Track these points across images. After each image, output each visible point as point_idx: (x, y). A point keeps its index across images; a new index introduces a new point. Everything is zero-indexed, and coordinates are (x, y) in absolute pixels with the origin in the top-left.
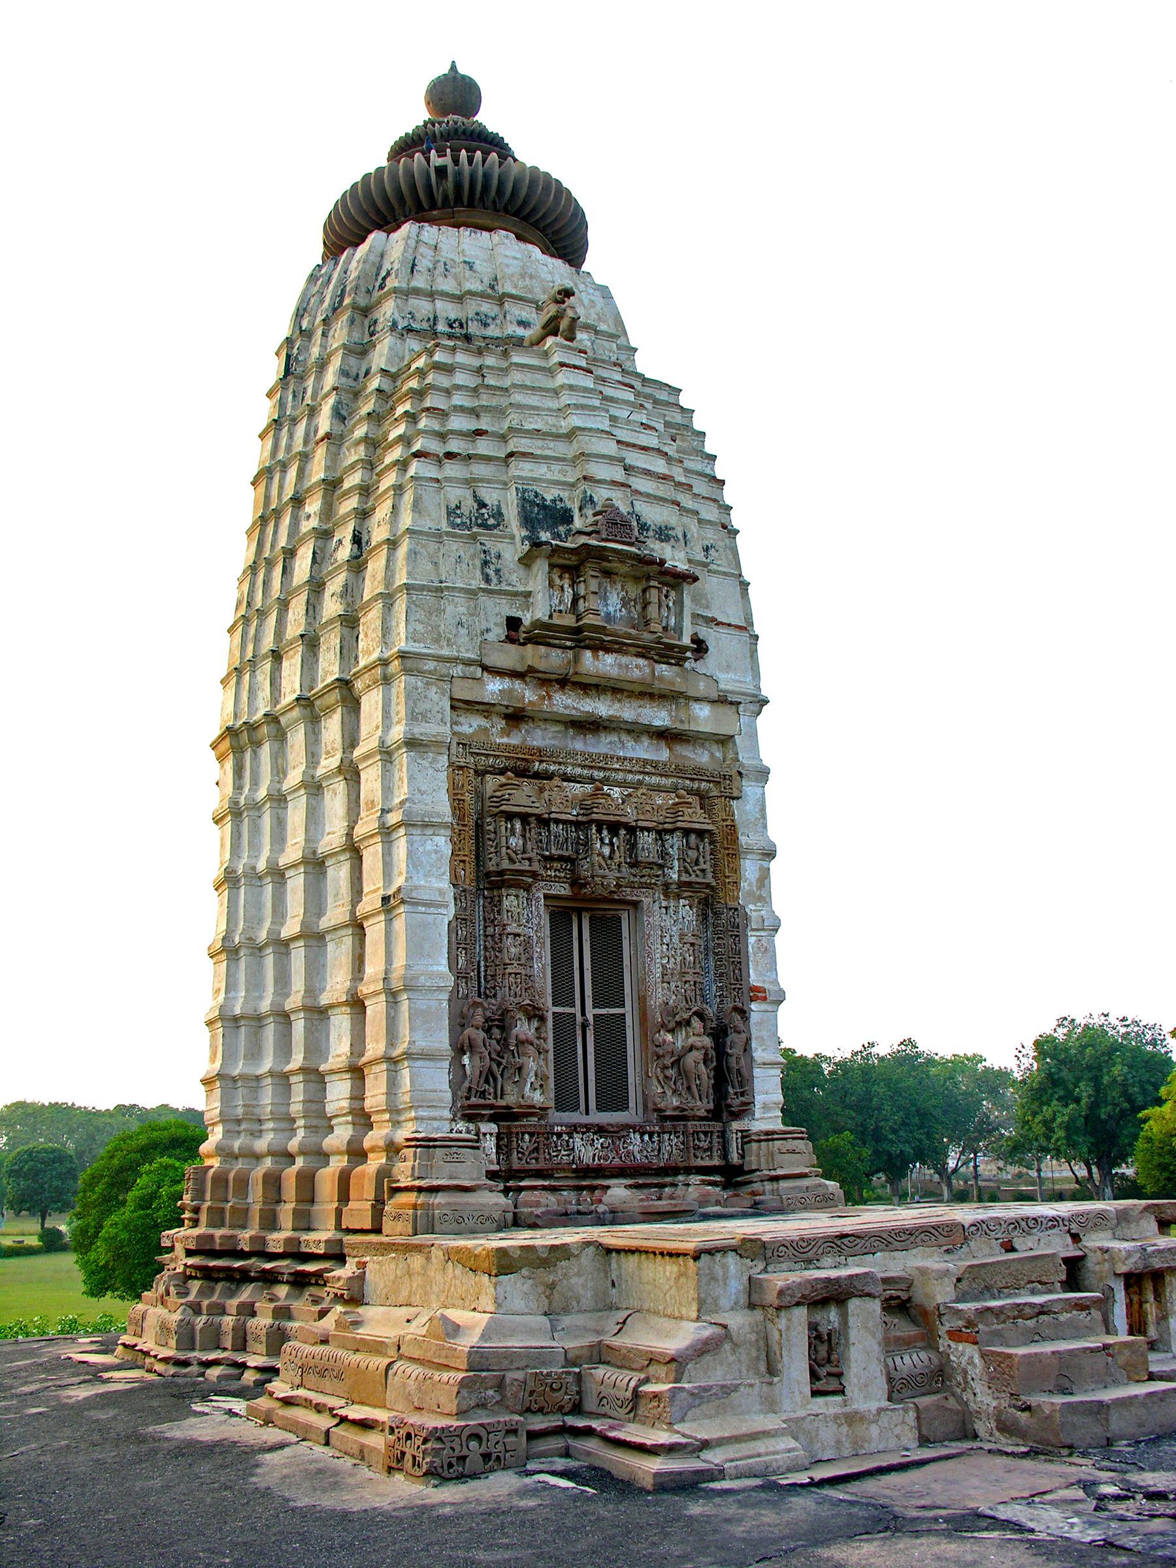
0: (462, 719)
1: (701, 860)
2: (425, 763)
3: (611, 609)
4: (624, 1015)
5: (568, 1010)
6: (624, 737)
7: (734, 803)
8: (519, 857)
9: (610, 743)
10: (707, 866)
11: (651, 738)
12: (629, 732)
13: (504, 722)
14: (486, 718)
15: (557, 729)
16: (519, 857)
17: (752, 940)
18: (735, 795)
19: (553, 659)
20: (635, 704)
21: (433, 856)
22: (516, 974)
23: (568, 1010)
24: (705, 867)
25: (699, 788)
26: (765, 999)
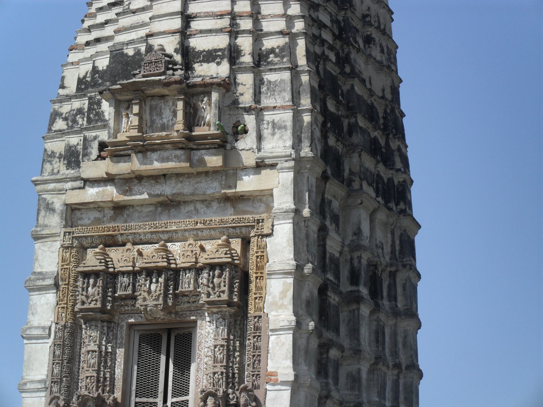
0: (84, 216)
1: (222, 284)
2: (45, 249)
3: (165, 121)
4: (188, 401)
5: (151, 400)
6: (199, 206)
7: (268, 240)
8: (90, 300)
9: (188, 212)
10: (226, 289)
11: (219, 203)
12: (203, 201)
13: (112, 212)
14: (100, 211)
15: (149, 209)
16: (90, 300)
17: (272, 338)
18: (266, 231)
19: (135, 164)
20: (193, 181)
21: (45, 306)
22: (91, 377)
23: (151, 400)
24: (223, 288)
25: (241, 232)
26: (277, 380)
